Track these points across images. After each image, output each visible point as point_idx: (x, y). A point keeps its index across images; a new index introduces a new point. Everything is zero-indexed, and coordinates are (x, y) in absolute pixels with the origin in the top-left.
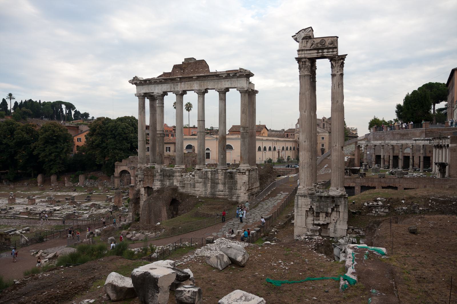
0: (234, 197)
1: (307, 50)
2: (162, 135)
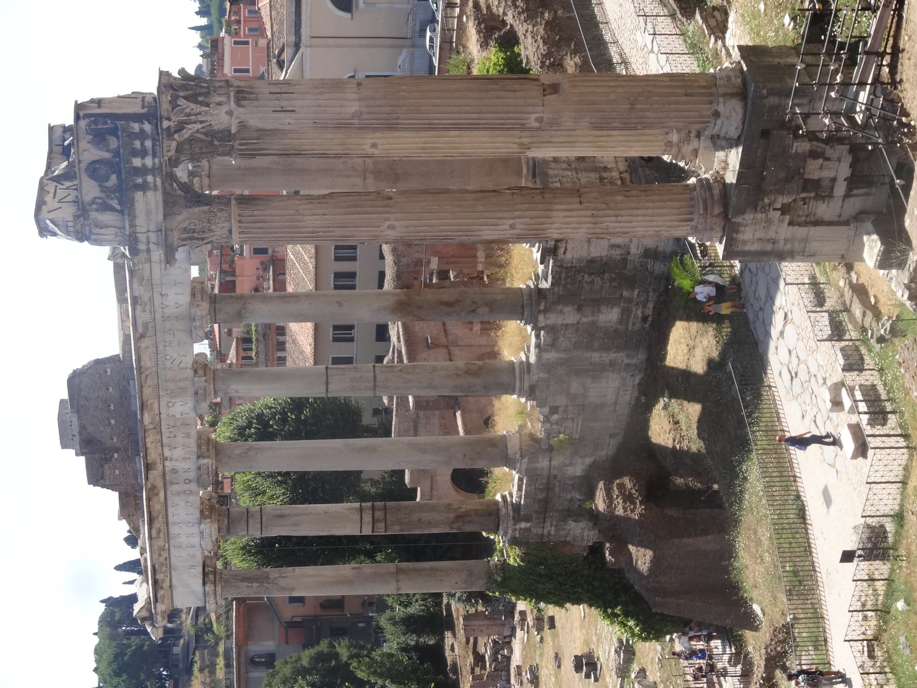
0: (656, 268)
1: (132, 225)
2: (379, 514)
